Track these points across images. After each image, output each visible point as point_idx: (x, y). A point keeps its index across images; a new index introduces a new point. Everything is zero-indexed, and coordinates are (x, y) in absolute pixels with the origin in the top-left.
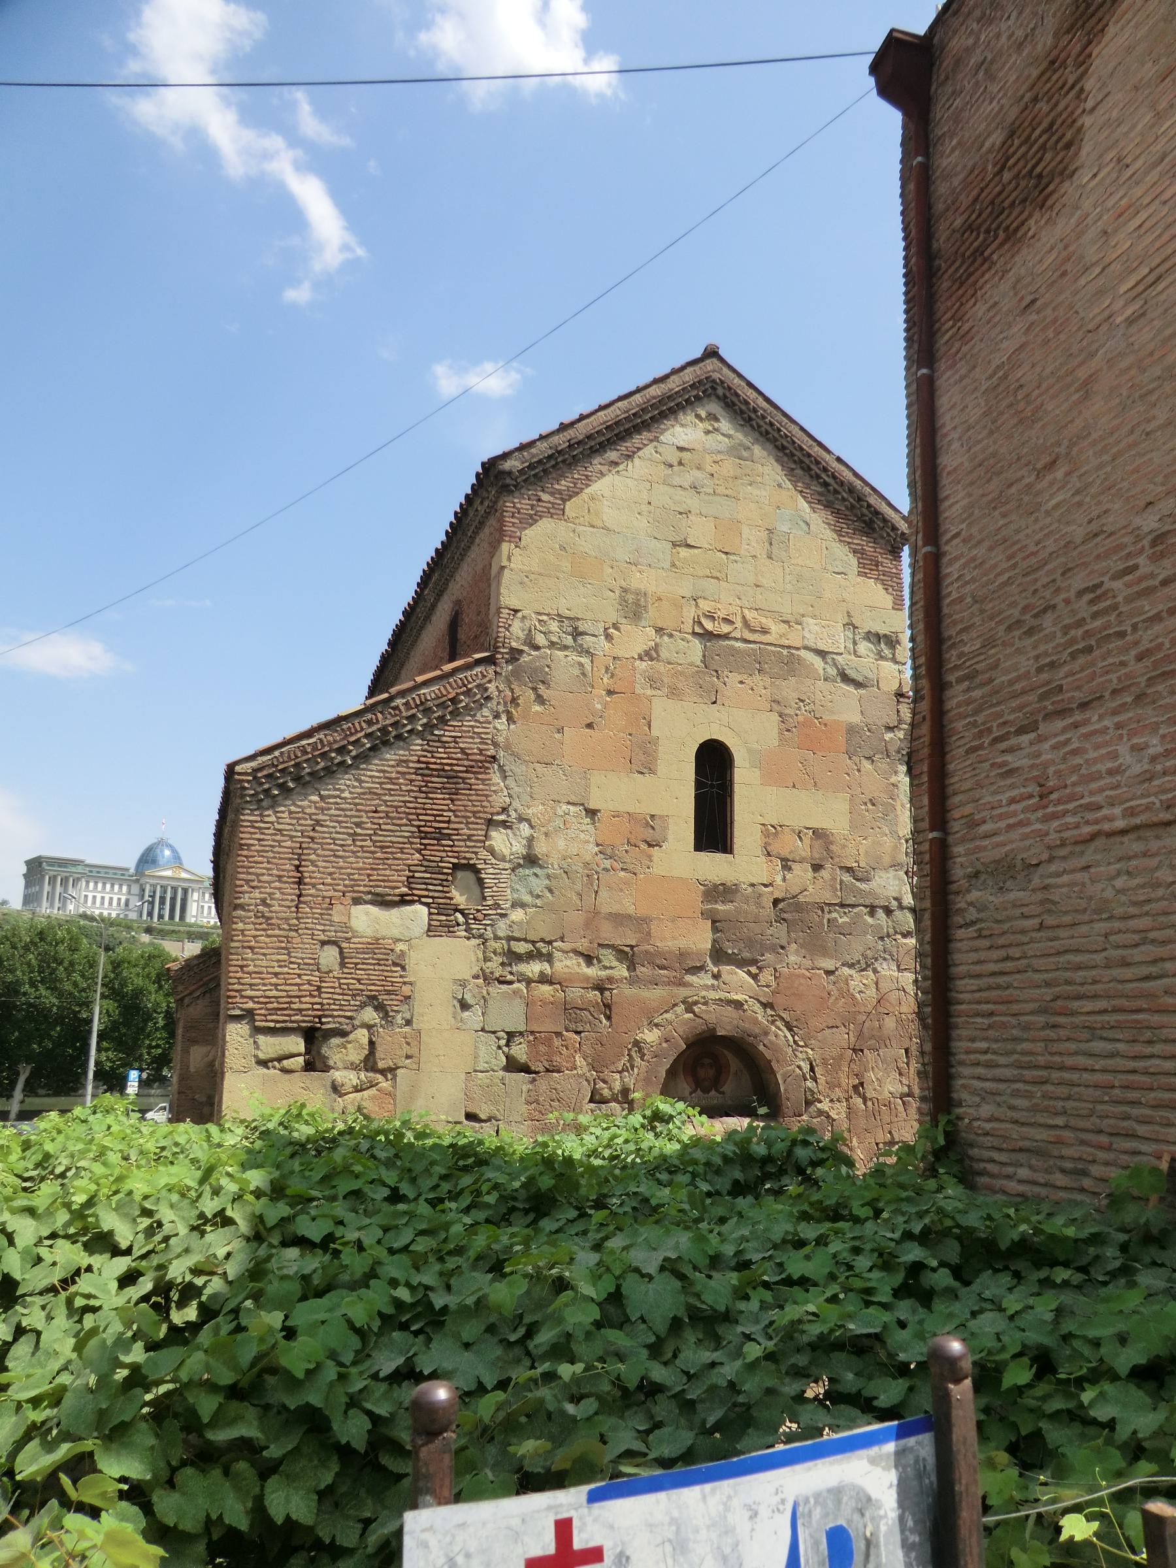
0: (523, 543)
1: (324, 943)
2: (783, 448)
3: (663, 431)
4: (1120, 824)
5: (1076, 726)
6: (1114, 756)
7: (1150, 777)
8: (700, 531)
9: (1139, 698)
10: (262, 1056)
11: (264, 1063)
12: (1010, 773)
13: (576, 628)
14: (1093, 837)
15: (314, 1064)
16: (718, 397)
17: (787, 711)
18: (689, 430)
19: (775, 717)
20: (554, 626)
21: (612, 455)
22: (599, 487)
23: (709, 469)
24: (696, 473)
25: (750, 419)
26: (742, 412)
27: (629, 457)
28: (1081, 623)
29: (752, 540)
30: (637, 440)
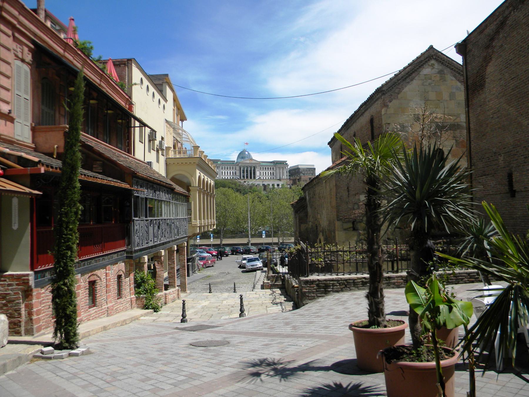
0: (389, 107)
1: (355, 204)
2: (452, 69)
3: (420, 72)
4: (491, 193)
5: (487, 178)
6: (490, 183)
7: (494, 187)
8: (432, 96)
9: (493, 176)
10: (344, 228)
11: (345, 230)
12: (480, 182)
13: (403, 126)
14: (488, 195)
15: (354, 229)
16: (434, 59)
17: (457, 139)
18: (427, 70)
19: (454, 141)
20: (399, 127)
21: (408, 80)
22: (406, 89)
23: (433, 79)
24: (430, 81)
25: (443, 63)
26: (440, 61)
27: (412, 80)
28: (487, 162)
29: (446, 96)
30: (414, 75)
